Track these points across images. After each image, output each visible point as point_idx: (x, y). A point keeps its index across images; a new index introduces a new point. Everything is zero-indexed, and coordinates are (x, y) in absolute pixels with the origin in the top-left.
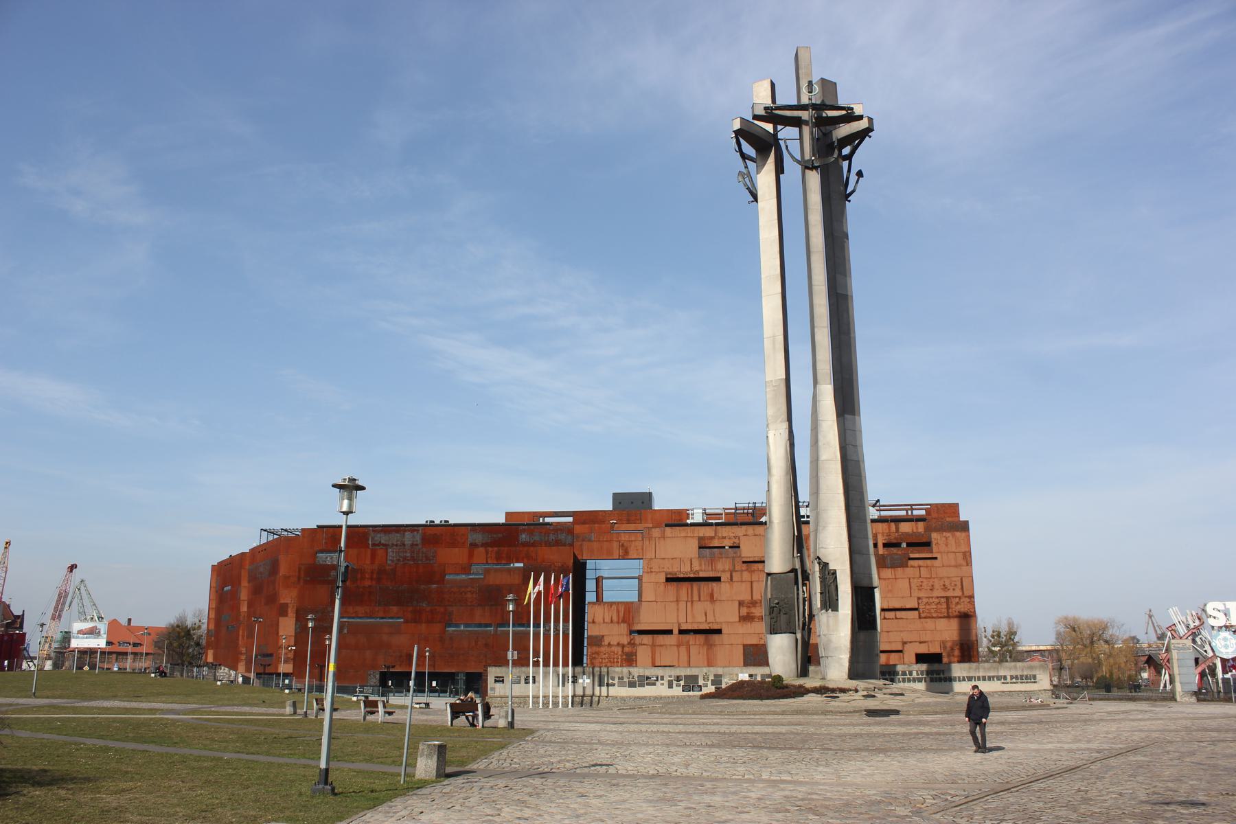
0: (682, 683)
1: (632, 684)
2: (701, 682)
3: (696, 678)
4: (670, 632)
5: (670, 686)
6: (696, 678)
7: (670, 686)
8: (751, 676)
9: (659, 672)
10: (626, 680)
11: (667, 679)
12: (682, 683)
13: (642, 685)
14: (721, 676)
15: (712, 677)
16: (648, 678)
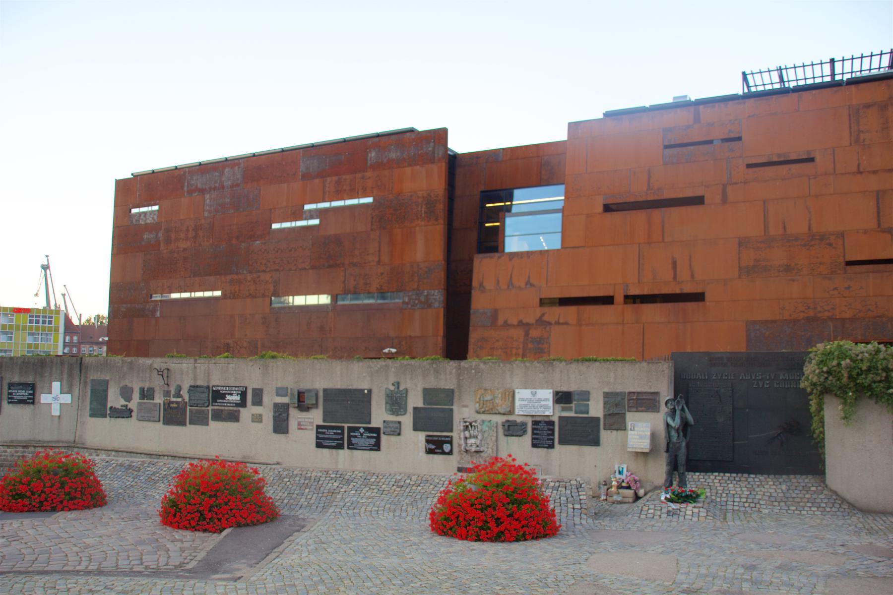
0: (316, 417)
1: (174, 416)
2: (379, 416)
3: (359, 401)
4: (608, 300)
5: (281, 426)
6: (359, 401)
7: (281, 426)
8: (563, 398)
9: (246, 373)
10: (159, 399)
11: (270, 399)
12: (316, 417)
13: (200, 420)
14: (449, 395)
15: (415, 400)
16: (218, 395)
